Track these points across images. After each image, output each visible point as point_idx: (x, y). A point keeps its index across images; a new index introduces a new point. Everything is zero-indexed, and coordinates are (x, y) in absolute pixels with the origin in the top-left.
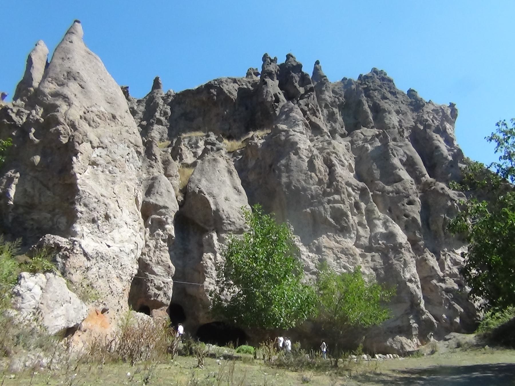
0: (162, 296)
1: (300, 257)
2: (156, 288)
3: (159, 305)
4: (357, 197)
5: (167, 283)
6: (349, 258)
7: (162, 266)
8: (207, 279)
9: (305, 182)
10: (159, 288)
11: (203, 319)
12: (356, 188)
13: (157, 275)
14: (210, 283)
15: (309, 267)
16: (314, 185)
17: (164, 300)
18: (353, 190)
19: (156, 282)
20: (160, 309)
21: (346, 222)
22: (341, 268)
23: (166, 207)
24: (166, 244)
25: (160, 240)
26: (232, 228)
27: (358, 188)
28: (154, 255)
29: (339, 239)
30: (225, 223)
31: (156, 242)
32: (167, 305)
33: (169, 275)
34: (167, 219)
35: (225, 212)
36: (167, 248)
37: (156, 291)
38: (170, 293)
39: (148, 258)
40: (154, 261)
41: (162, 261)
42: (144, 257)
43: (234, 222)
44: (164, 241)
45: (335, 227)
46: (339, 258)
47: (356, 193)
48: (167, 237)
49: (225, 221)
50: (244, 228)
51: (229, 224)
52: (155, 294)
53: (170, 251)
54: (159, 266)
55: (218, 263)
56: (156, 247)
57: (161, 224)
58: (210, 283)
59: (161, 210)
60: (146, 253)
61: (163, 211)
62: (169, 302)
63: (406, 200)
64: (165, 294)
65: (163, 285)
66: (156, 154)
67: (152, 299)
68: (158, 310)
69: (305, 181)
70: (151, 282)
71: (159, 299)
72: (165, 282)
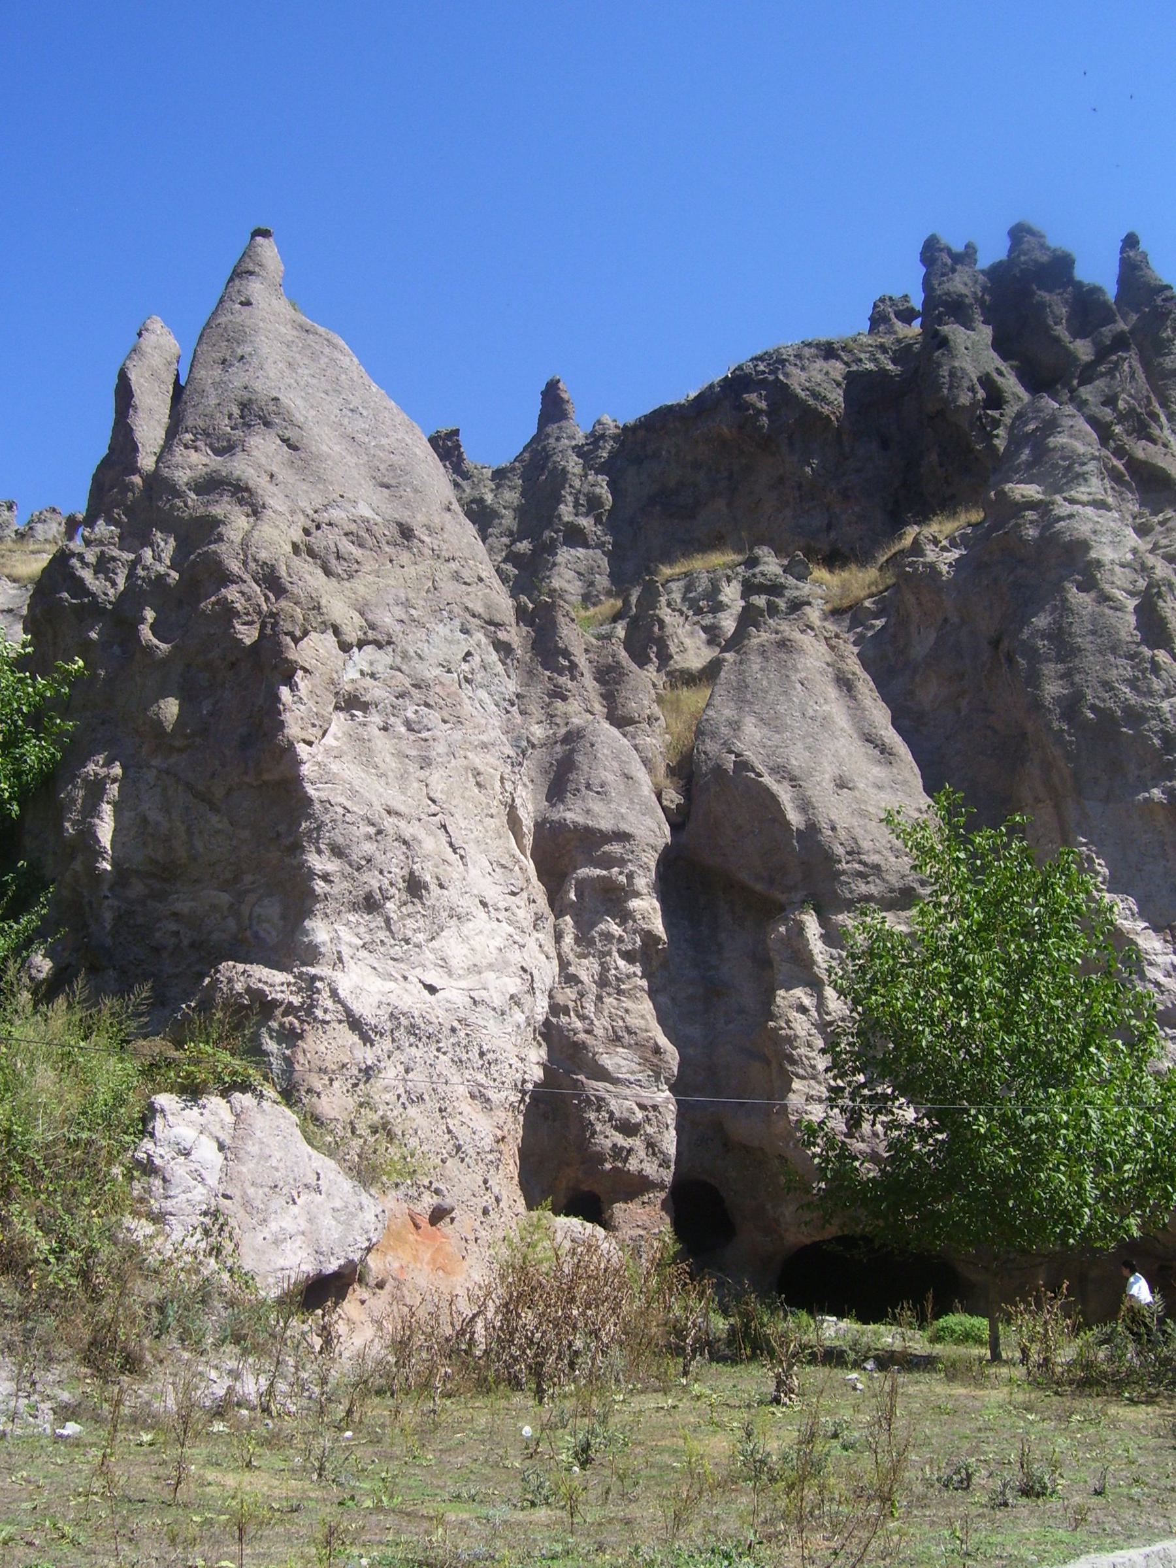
0: (642, 1154)
1: (1143, 977)
2: (616, 1128)
3: (637, 1187)
5: (655, 1108)
7: (629, 1047)
8: (796, 1084)
9: (1134, 688)
10: (628, 1128)
11: (797, 1228)
13: (615, 1081)
14: (809, 1098)
17: (651, 1169)
19: (614, 1104)
20: (639, 1201)
23: (623, 837)
24: (638, 969)
25: (615, 954)
26: (873, 889)
28: (598, 1011)
30: (844, 872)
31: (601, 964)
32: (661, 1186)
33: (657, 1080)
34: (630, 876)
35: (842, 834)
36: (644, 983)
37: (620, 1140)
38: (669, 1143)
39: (579, 1024)
40: (599, 1032)
41: (629, 1031)
42: (564, 1019)
43: (877, 868)
44: (628, 956)
48: (639, 943)
49: (844, 866)
50: (916, 885)
51: (860, 875)
52: (617, 1151)
53: (652, 993)
54: (620, 1050)
55: (831, 1023)
56: (602, 982)
57: (612, 899)
58: (809, 1098)
59: (607, 848)
60: (571, 1005)
61: (615, 848)
62: (668, 1176)
64: (651, 1145)
65: (640, 1115)
66: (571, 649)
67: (608, 1166)
68: (630, 1205)
69: (1132, 683)
70: (598, 1110)
71: (633, 1165)
72: (646, 1102)
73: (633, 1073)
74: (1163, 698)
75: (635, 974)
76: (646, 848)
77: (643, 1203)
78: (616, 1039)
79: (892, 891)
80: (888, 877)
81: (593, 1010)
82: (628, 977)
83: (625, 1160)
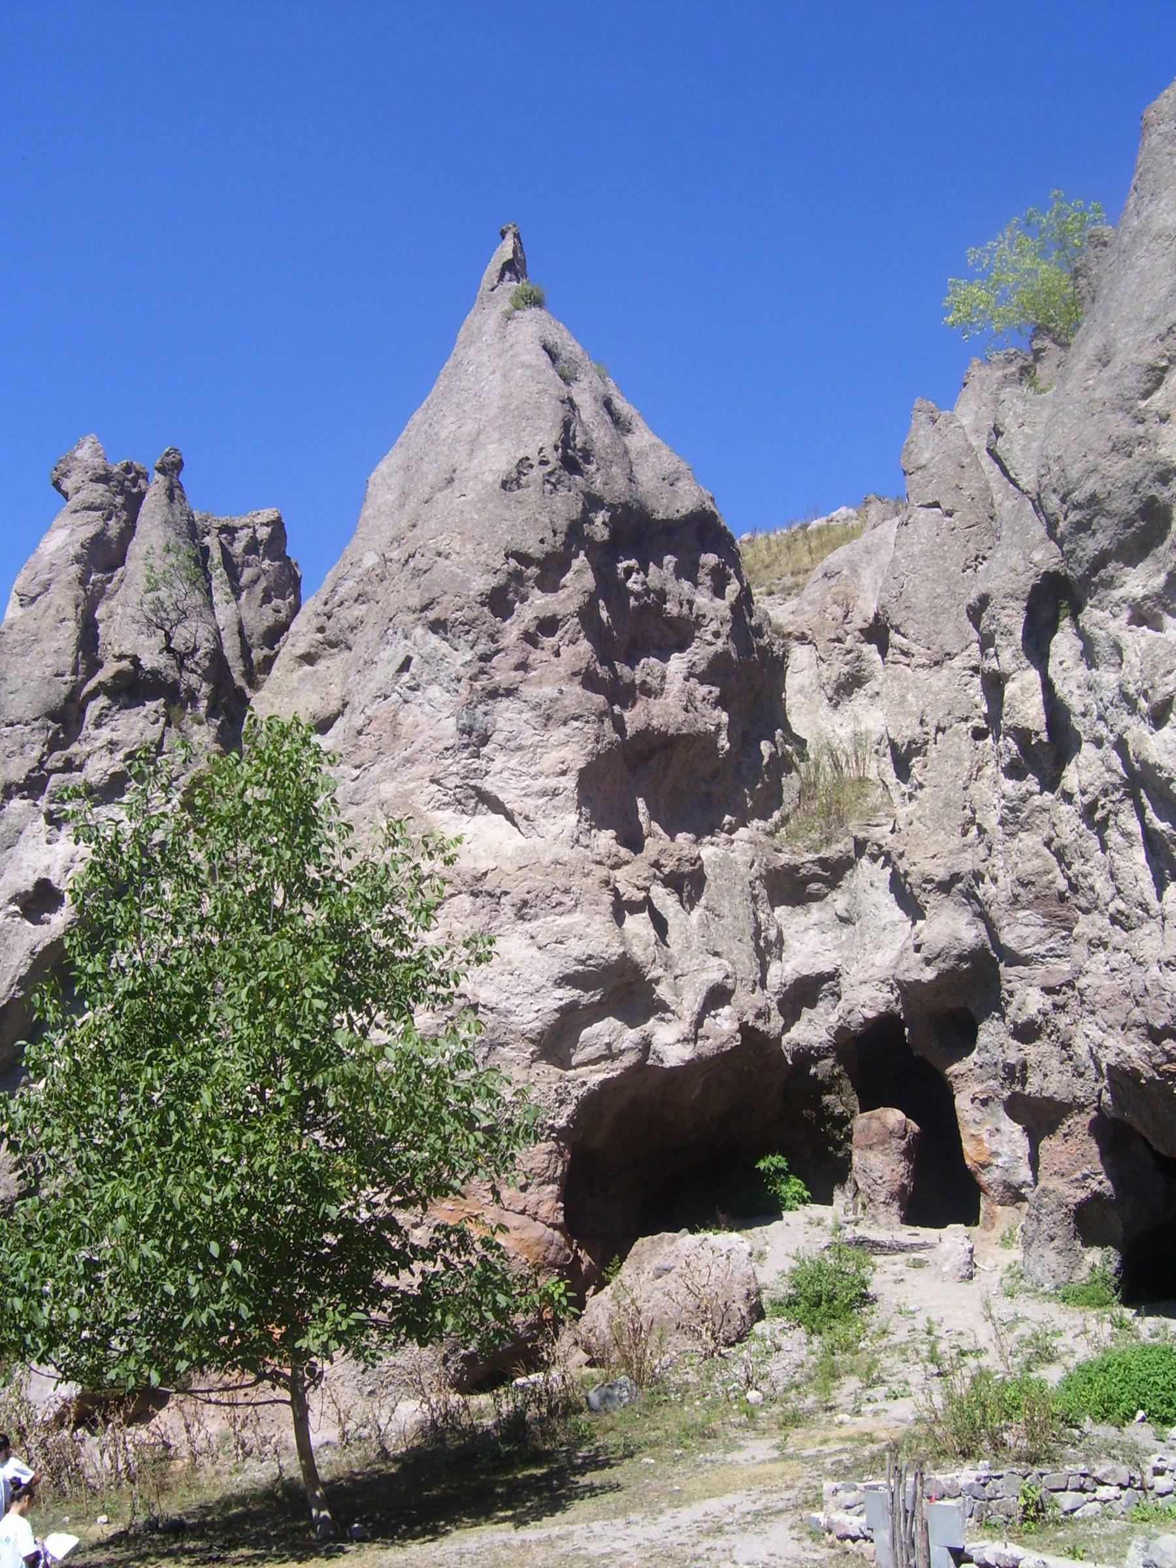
10: (1027, 1032)
13: (1025, 961)
32: (1082, 1108)
41: (1024, 885)
43: (1093, 499)
60: (981, 867)
72: (1053, 982)
73: (1041, 941)
75: (1032, 794)
76: (1004, 602)
77: (1065, 1135)
81: (1001, 864)
82: (1023, 800)
83: (1024, 1081)
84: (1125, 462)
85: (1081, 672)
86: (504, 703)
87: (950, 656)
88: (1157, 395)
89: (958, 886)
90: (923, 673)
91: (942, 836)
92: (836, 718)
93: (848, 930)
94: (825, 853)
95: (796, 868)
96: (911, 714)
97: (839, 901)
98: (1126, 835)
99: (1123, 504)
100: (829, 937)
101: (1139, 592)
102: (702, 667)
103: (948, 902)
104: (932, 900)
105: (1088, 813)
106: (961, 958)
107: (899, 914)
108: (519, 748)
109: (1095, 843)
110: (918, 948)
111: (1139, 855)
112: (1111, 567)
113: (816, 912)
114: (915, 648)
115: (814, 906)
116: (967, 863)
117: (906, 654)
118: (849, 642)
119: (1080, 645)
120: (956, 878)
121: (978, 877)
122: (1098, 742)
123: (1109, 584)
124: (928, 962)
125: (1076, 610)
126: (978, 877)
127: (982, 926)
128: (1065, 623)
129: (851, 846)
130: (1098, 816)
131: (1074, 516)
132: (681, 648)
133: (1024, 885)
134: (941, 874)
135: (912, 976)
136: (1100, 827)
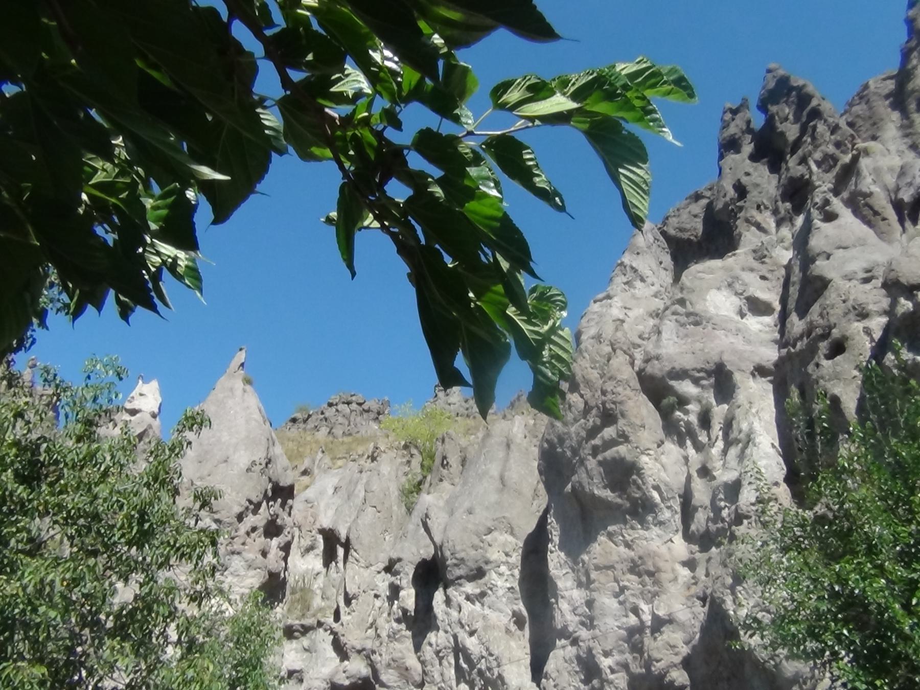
4: (710, 397)
6: (643, 584)
12: (702, 374)
15: (565, 627)
16: (576, 420)
18: (696, 382)
21: (639, 488)
22: (627, 616)
23: (399, 560)
24: (403, 626)
27: (706, 371)
29: (629, 535)
30: (448, 566)
35: (451, 543)
36: (409, 633)
41: (393, 660)
43: (462, 559)
44: (398, 621)
45: (619, 506)
46: (623, 589)
47: (703, 387)
50: (483, 565)
51: (456, 565)
54: (390, 671)
55: (440, 651)
63: (824, 346)
73: (396, 682)
74: (573, 424)
78: (389, 665)
79: (472, 570)
80: (468, 564)
82: (399, 631)
84: (474, 552)
85: (443, 606)
86: (236, 557)
87: (371, 565)
88: (489, 536)
89: (367, 655)
90: (362, 570)
91: (358, 632)
92: (302, 561)
93: (306, 655)
94: (304, 622)
95: (292, 626)
96: (355, 584)
97: (305, 642)
98: (450, 663)
99: (473, 565)
100: (299, 655)
101: (470, 592)
102: (282, 544)
103: (359, 658)
104: (353, 656)
105: (437, 653)
106: (359, 679)
107: (334, 654)
108: (238, 575)
109: (437, 662)
110: (344, 672)
111: (453, 671)
112: (462, 581)
113: (294, 644)
114: (361, 560)
115: (294, 641)
116: (369, 645)
117: (357, 561)
118: (314, 532)
119: (445, 598)
120: (364, 649)
121: (374, 652)
122: (446, 632)
123: (460, 585)
124: (348, 678)
125: (446, 588)
126: (374, 652)
127: (370, 669)
128: (441, 589)
129: (316, 622)
130: (441, 654)
131: (454, 561)
132: (277, 535)
133: (393, 660)
134: (359, 647)
135: (341, 682)
136: (441, 659)
